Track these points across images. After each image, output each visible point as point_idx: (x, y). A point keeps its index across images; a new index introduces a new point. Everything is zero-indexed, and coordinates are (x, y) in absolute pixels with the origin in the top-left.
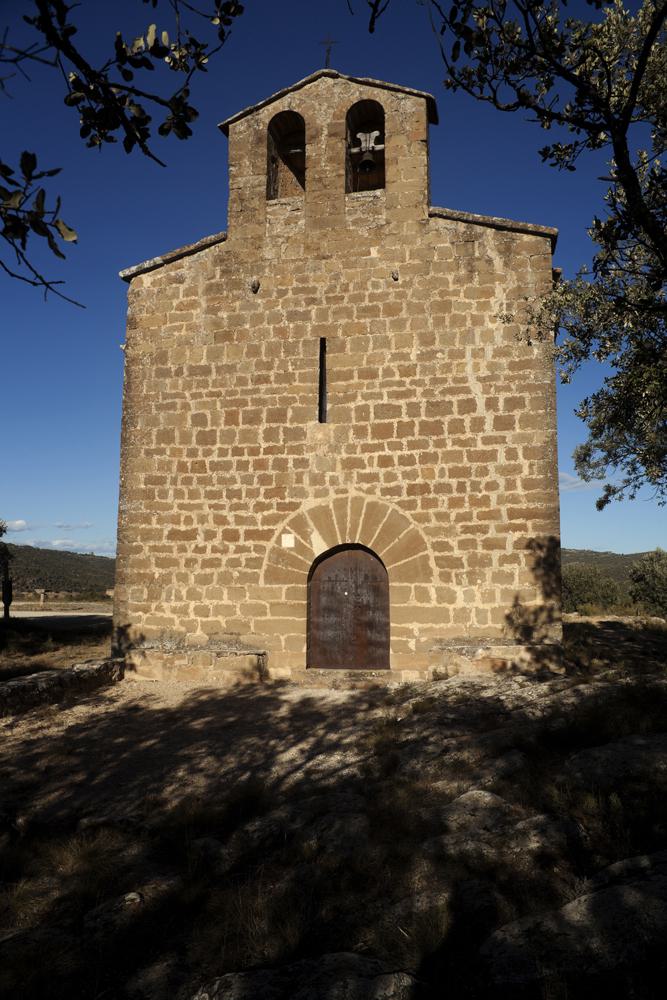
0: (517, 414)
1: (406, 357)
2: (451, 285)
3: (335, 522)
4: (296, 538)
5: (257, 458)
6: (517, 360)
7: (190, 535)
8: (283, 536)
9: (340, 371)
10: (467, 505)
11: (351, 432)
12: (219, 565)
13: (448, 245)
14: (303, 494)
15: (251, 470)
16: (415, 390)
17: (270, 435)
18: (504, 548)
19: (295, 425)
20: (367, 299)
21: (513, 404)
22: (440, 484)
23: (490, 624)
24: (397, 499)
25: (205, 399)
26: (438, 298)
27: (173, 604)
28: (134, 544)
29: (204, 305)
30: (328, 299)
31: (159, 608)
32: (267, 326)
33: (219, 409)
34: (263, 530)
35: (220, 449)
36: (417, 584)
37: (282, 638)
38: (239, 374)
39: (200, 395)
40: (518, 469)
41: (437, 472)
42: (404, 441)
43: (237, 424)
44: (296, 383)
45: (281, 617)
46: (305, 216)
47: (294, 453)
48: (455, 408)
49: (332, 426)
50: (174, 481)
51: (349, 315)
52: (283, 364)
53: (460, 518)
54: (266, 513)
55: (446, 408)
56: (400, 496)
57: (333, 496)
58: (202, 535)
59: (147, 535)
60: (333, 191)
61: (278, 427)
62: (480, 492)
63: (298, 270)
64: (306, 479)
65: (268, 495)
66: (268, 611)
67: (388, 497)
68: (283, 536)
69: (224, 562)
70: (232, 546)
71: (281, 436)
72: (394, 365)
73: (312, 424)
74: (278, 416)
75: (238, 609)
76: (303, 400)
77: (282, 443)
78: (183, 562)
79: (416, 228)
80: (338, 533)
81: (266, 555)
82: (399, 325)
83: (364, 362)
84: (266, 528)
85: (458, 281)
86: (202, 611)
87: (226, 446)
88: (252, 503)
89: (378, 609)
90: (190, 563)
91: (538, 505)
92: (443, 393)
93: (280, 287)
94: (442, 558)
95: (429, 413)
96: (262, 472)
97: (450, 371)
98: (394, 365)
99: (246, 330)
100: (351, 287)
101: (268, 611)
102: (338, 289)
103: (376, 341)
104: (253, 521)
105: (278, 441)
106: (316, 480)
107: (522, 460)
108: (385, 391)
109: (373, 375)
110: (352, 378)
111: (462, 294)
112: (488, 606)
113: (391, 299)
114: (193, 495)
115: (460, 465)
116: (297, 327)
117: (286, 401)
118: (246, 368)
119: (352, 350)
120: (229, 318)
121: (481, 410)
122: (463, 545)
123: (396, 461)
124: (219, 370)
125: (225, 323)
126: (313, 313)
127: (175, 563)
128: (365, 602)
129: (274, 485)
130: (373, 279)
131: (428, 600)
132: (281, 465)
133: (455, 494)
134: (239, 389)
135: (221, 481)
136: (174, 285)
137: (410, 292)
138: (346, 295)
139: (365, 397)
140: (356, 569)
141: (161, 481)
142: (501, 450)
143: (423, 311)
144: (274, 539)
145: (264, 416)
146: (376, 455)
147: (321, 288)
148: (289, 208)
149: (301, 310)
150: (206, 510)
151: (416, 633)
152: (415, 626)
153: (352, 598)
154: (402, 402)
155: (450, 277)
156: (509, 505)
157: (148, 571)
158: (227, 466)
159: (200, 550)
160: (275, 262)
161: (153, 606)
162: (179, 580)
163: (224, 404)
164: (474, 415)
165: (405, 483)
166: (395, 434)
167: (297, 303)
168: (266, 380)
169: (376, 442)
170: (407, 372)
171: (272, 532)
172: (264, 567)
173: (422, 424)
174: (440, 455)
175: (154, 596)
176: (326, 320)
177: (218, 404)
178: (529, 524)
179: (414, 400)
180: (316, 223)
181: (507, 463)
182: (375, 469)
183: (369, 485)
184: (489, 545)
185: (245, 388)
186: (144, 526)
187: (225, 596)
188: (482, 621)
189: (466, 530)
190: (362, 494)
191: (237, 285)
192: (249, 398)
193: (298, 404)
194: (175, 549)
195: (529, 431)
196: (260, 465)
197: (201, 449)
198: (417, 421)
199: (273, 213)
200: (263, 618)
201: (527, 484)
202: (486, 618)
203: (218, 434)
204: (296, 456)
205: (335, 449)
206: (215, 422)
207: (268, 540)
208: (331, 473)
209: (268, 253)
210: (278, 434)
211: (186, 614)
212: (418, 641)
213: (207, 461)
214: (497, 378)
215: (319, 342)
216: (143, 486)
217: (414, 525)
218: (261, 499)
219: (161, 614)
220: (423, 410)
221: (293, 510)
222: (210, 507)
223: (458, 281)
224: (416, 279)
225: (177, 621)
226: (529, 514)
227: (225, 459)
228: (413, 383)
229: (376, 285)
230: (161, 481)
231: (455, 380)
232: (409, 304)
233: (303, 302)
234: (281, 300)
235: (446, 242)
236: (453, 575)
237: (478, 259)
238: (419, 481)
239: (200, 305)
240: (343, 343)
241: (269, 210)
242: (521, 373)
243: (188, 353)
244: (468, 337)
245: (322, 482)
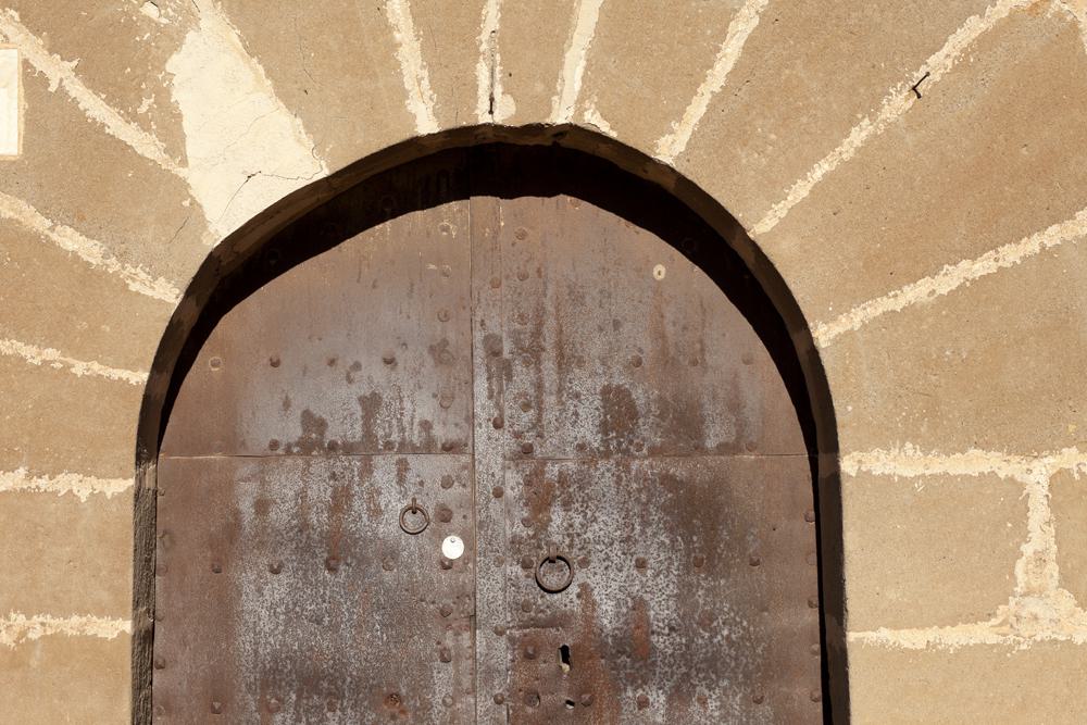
4: (33, 81)
89: (713, 666)
128: (608, 615)
140: (533, 355)
153: (497, 587)
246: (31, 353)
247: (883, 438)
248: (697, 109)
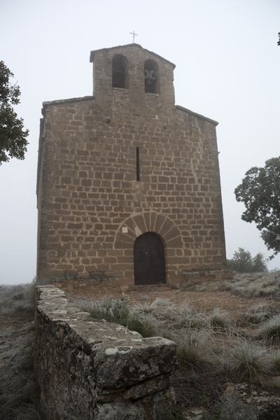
0: (208, 185)
7: (80, 226)
11: (150, 186)
12: (93, 241)
14: (131, 210)
15: (108, 199)
17: (116, 184)
21: (207, 181)
24: (168, 214)
27: (71, 259)
31: (64, 261)
35: (93, 188)
37: (124, 273)
40: (209, 206)
42: (170, 192)
43: (101, 178)
47: (127, 193)
48: (188, 181)
49: (143, 183)
50: (71, 201)
53: (191, 223)
57: (144, 212)
59: (57, 226)
64: (132, 204)
71: (121, 185)
74: (119, 176)
76: (130, 171)
78: (76, 238)
82: (167, 147)
88: (109, 213)
90: (79, 239)
94: (186, 238)
106: (137, 204)
107: (211, 202)
108: (162, 171)
109: (158, 164)
113: (163, 137)
114: (81, 208)
120: (97, 132)
121: (197, 183)
122: (194, 233)
124: (92, 153)
125: (95, 134)
126: (134, 137)
127: (72, 239)
131: (181, 254)
132: (121, 197)
133: (189, 214)
135: (94, 202)
139: (155, 173)
141: (64, 200)
144: (119, 229)
145: (113, 176)
149: (128, 134)
150: (87, 215)
151: (178, 268)
154: (169, 176)
158: (97, 196)
159: (83, 233)
168: (114, 160)
171: (118, 226)
172: (115, 241)
175: (61, 254)
176: (139, 140)
177: (92, 169)
182: (160, 202)
186: (55, 221)
187: (97, 254)
189: (194, 227)
194: (72, 233)
195: (212, 192)
197: (84, 188)
198: (174, 184)
205: (144, 192)
206: (91, 175)
207: (116, 229)
211: (78, 263)
213: (87, 193)
216: (54, 202)
217: (175, 225)
218: (113, 211)
219: (64, 264)
220: (177, 180)
222: (89, 214)
224: (172, 130)
225: (73, 267)
226: (214, 222)
230: (64, 200)
231: (187, 170)
238: (176, 208)
240: (146, 151)
241: (114, 91)
243: (77, 144)
244: (191, 155)
245: (139, 206)
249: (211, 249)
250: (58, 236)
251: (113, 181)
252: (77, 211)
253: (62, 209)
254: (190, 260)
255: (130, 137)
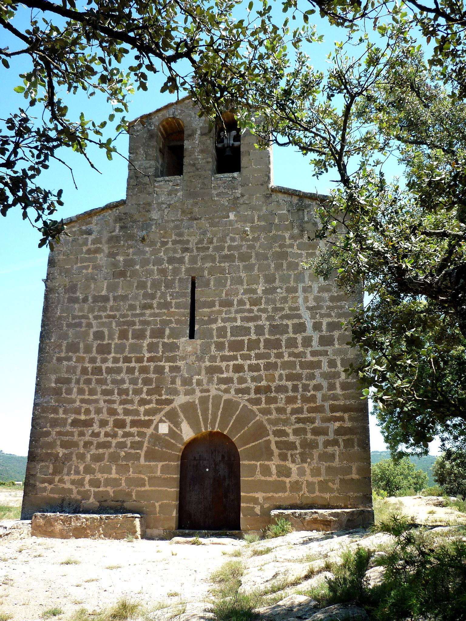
1: (254, 291)
2: (287, 240)
3: (200, 414)
4: (169, 426)
5: (141, 365)
6: (336, 295)
7: (88, 423)
8: (160, 424)
9: (205, 301)
10: (299, 401)
11: (213, 347)
13: (285, 212)
14: (175, 392)
15: (137, 374)
16: (261, 316)
17: (152, 347)
18: (328, 435)
19: (171, 340)
20: (226, 250)
21: (332, 326)
22: (279, 386)
23: (317, 493)
24: (246, 397)
25: (104, 320)
26: (278, 249)
27: (73, 477)
28: (45, 429)
29: (106, 251)
30: (197, 248)
31: (61, 481)
32: (152, 267)
33: (114, 328)
34: (145, 420)
35: (113, 357)
36: (261, 462)
37: (157, 505)
38: (130, 302)
39: (100, 317)
41: (277, 376)
42: (253, 353)
43: (127, 339)
44: (173, 310)
45: (157, 488)
46: (182, 190)
48: (290, 329)
49: (199, 342)
50: (78, 382)
51: (213, 260)
52: (163, 295)
53: (295, 411)
54: (147, 407)
55: (283, 329)
56: (249, 395)
57: (198, 394)
58: (98, 423)
59: (55, 423)
60: (203, 173)
61: (159, 342)
62: (309, 392)
63: (176, 227)
64: (178, 381)
65: (149, 393)
66: (147, 483)
67: (240, 395)
68: (160, 424)
69: (114, 445)
70: (120, 432)
71: (161, 349)
72: (245, 297)
73: (183, 340)
75: (123, 481)
76: (178, 322)
77: (161, 353)
78: (82, 444)
79: (263, 199)
80: (202, 422)
81: (147, 439)
82: (249, 268)
83: (224, 295)
84: (147, 418)
85: (292, 237)
86: (95, 483)
87: (118, 356)
88: (137, 399)
90: (87, 445)
91: (353, 402)
92: (282, 318)
93: (163, 239)
94: (281, 442)
95: (271, 333)
96: (145, 376)
97: (286, 302)
98: (245, 297)
99: (137, 269)
100: (215, 240)
101: (147, 483)
102: (205, 241)
103: (232, 279)
104: (137, 413)
105: (158, 352)
106: (186, 382)
108: (238, 316)
110: (214, 306)
111: (295, 247)
112: (315, 480)
113: (244, 249)
114: (92, 392)
115: (294, 372)
116: (174, 269)
117: (166, 323)
118: (136, 298)
119: (214, 286)
120: (124, 260)
121: (309, 331)
122: (296, 432)
123: (246, 368)
124: (115, 298)
125: (121, 264)
126: (187, 259)
127: (75, 445)
129: (154, 386)
130: (231, 235)
132: (159, 370)
133: (290, 394)
134: (129, 313)
135: (114, 382)
136: (85, 236)
137: (257, 245)
138: (211, 246)
139: (224, 320)
140: (215, 451)
141: (68, 381)
142: (324, 361)
143: (267, 259)
144: (153, 426)
145: (148, 333)
146: (231, 363)
147: (193, 240)
148: (171, 184)
149: (178, 256)
150: (102, 404)
151: (261, 500)
152: (260, 495)
154: (251, 324)
155: (287, 235)
156: (331, 402)
157: (54, 451)
158: (119, 371)
159: (96, 435)
160: (160, 221)
161: (57, 479)
162: (77, 458)
163: (118, 324)
164: (304, 334)
165: (253, 385)
166: (246, 349)
167: (175, 251)
168: (150, 307)
169: (231, 353)
170: (255, 302)
171: (151, 421)
172: (145, 449)
173: (266, 341)
174: (279, 364)
178: (346, 416)
179: (260, 323)
180: (190, 194)
181: (329, 370)
182: (231, 374)
183: (226, 386)
184: (316, 432)
185: (134, 312)
186: (52, 415)
187: (114, 471)
188: (312, 491)
189: (299, 420)
190: (220, 393)
191: (131, 237)
192: (137, 320)
193: (174, 325)
194: (76, 434)
196: (144, 370)
197: (99, 357)
199: (160, 187)
200: (143, 489)
201: (344, 386)
202: (314, 489)
203: (113, 346)
204: (172, 364)
205: (200, 359)
206: (111, 337)
207: (148, 428)
208: (197, 377)
209: (155, 215)
210: (158, 347)
211: (83, 485)
212: (262, 507)
213: (104, 366)
214: (320, 307)
215: (190, 280)
216: (53, 385)
218: (144, 396)
219: (63, 485)
220: (266, 331)
221: (168, 405)
222: (105, 401)
223: (292, 237)
226: (345, 409)
227: (117, 365)
228: (259, 310)
229: (233, 240)
230: (68, 381)
231: (291, 309)
232: (257, 254)
233: (179, 251)
234: (163, 249)
235: (284, 210)
236: (289, 455)
237: (307, 222)
238: (264, 383)
239: (103, 251)
240: (209, 281)
242: (339, 304)
243: (92, 286)
245: (191, 384)
246: (169, 451)
247: (244, 460)
248: (228, 429)
249: (336, 463)
250: (55, 441)
251: (145, 343)
252: (86, 397)
253: (64, 395)
254: (288, 485)
255: (181, 261)
